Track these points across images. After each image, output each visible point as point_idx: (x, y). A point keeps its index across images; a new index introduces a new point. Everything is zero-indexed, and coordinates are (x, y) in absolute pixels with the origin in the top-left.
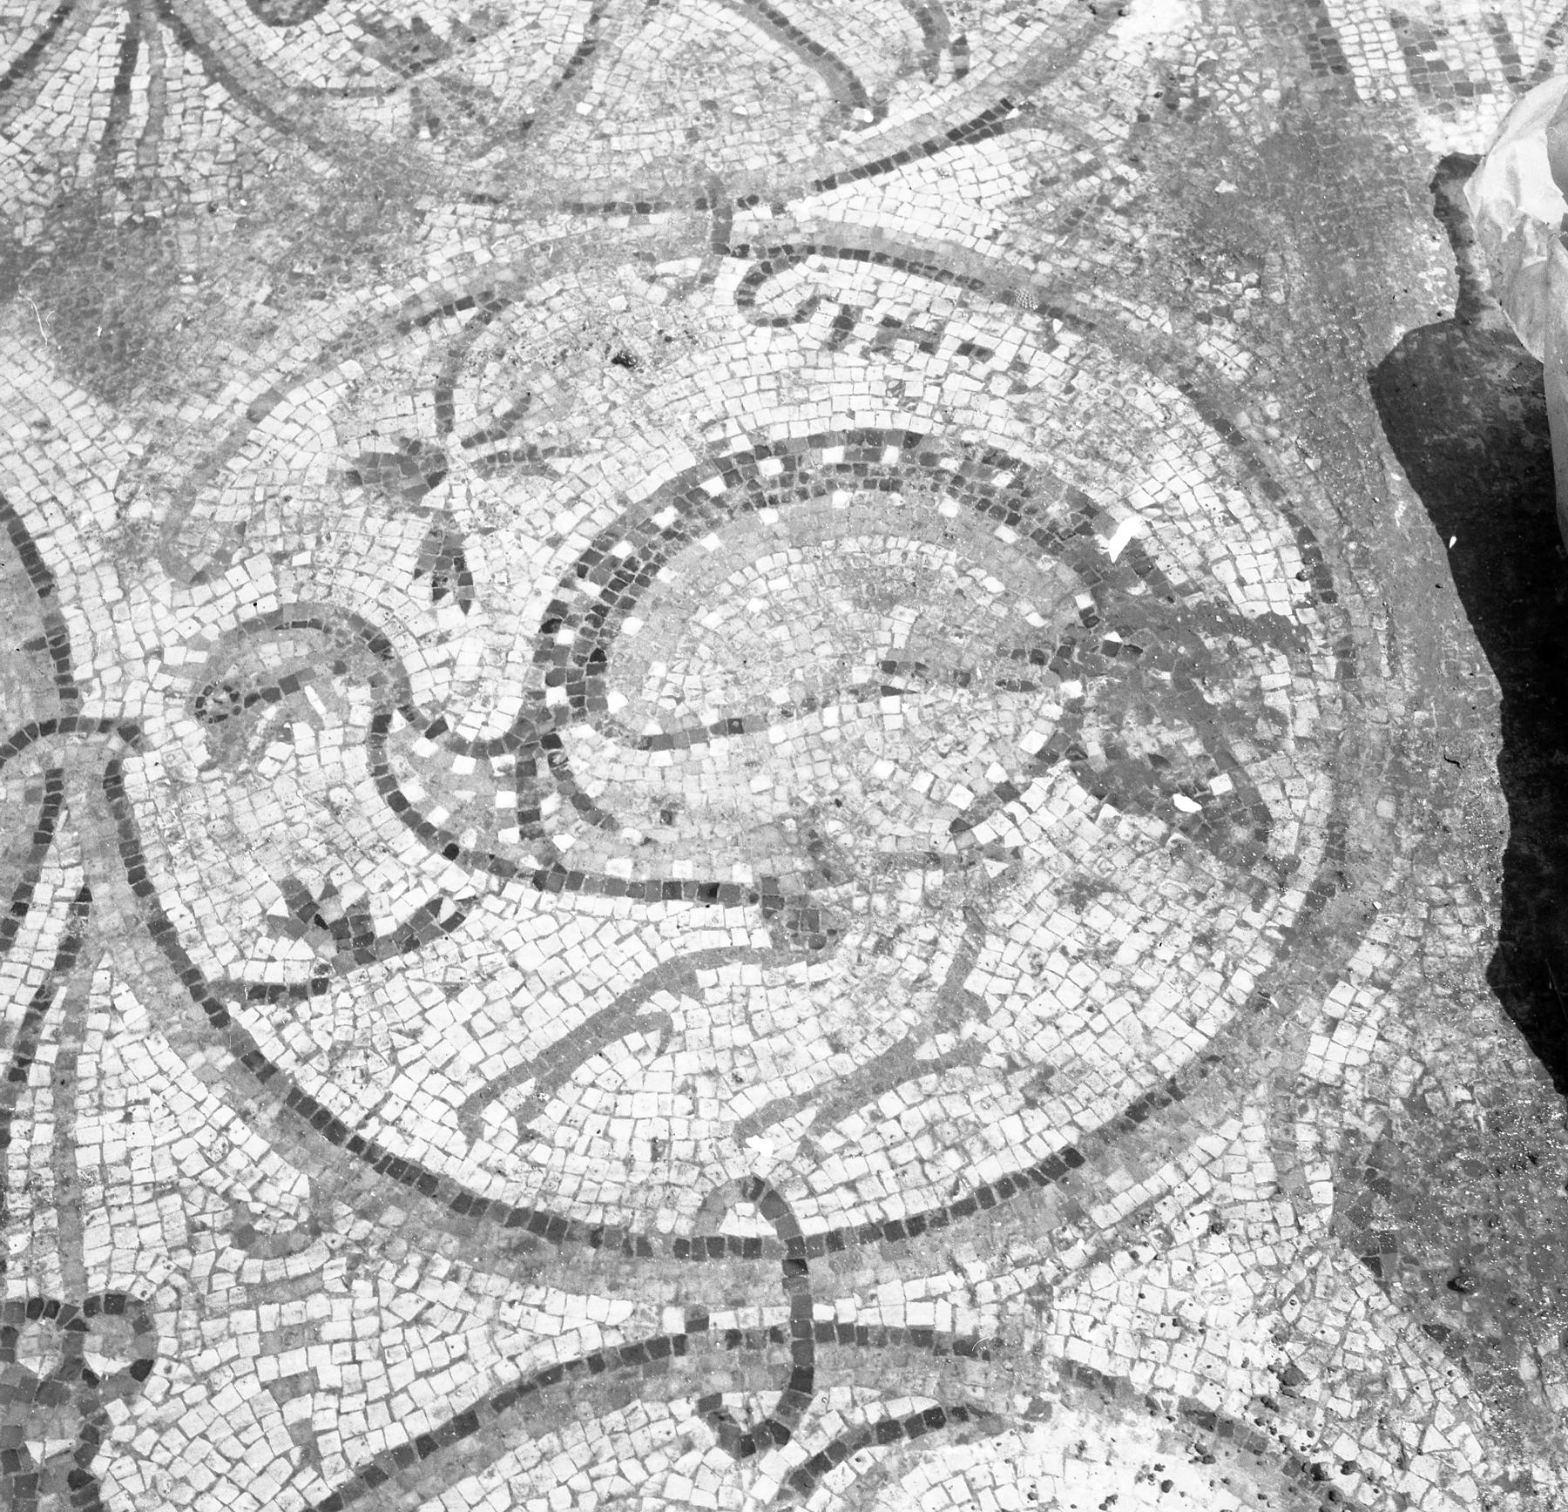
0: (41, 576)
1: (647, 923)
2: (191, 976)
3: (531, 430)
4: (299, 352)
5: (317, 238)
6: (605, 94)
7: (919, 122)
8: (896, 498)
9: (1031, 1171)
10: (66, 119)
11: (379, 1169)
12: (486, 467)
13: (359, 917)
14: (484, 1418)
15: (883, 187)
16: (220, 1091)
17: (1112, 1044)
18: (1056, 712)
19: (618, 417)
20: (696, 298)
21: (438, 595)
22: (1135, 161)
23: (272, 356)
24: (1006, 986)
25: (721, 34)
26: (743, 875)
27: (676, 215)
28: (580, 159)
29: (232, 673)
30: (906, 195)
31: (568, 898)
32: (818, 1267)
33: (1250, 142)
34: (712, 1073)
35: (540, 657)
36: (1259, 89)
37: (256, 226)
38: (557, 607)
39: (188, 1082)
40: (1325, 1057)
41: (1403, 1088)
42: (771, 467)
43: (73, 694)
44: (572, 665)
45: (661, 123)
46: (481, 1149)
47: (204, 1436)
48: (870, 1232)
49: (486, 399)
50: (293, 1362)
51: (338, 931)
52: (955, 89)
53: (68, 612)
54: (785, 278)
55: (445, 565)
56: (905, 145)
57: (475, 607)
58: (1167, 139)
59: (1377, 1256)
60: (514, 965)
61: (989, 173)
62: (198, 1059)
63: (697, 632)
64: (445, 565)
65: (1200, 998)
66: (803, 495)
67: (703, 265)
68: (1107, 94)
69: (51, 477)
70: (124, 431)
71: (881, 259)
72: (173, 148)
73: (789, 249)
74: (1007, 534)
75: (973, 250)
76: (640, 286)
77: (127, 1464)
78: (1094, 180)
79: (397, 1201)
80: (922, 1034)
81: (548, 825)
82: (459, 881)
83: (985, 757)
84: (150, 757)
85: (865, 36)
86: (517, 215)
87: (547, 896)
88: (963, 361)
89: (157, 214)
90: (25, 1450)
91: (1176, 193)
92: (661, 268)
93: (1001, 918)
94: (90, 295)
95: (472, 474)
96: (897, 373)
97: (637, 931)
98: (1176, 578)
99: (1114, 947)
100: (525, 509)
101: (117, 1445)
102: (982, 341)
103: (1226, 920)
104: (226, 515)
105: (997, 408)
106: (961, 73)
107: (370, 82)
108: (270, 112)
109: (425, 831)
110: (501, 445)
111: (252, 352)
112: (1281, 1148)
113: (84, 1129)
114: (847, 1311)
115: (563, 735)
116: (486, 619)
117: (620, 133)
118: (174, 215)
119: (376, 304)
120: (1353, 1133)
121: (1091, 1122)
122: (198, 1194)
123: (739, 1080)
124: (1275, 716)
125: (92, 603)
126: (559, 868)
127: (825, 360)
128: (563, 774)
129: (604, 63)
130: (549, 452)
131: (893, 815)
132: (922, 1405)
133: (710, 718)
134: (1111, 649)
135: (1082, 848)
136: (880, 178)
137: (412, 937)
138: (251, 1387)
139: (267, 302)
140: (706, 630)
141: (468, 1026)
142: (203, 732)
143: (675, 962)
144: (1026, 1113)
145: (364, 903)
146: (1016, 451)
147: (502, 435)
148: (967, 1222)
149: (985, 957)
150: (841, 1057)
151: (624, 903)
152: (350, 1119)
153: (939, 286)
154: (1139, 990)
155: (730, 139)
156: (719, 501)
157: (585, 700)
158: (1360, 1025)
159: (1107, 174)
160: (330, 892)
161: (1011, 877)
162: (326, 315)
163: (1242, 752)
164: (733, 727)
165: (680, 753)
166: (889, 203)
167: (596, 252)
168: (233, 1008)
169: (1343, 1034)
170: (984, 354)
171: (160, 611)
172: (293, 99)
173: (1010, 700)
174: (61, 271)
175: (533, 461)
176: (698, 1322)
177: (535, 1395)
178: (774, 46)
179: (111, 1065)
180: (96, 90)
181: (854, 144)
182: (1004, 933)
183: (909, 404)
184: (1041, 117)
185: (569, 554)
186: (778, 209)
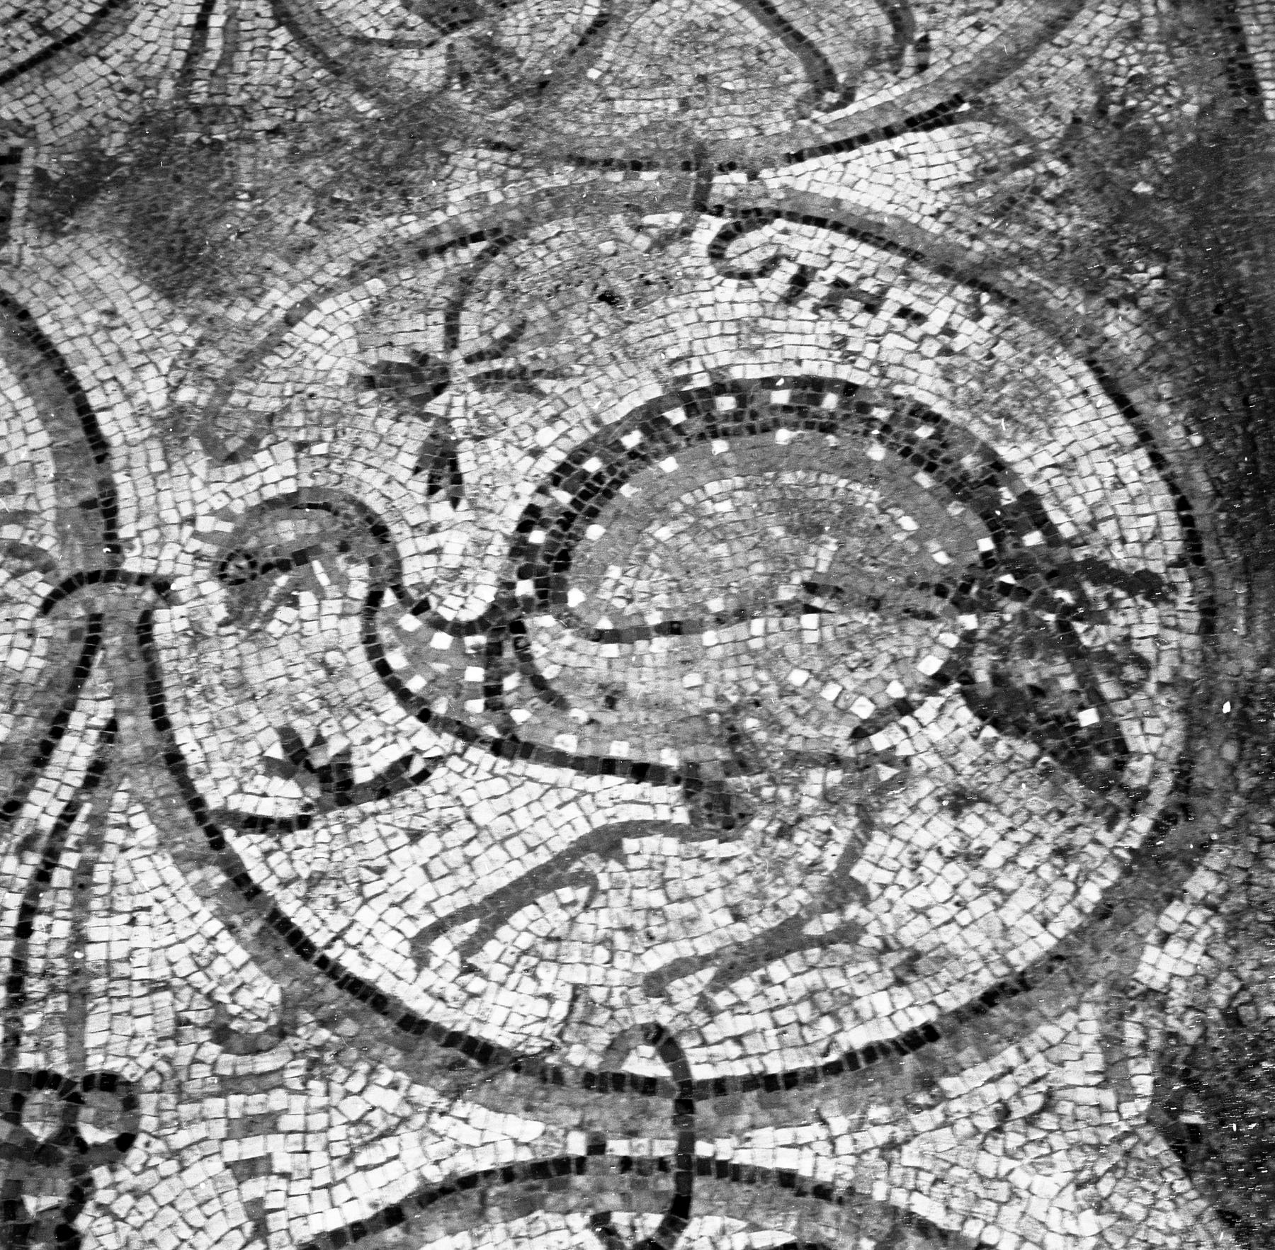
0: (99, 445)
1: (584, 793)
2: (197, 803)
3: (524, 353)
4: (333, 268)
5: (357, 169)
6: (612, 62)
7: (881, 108)
8: (831, 440)
9: (894, 1042)
10: (152, 48)
11: (340, 986)
12: (484, 382)
13: (342, 764)
15: (846, 163)
16: (212, 905)
17: (975, 937)
18: (952, 640)
19: (600, 348)
20: (676, 249)
21: (432, 490)
22: (1065, 159)
23: (310, 269)
24: (886, 877)
25: (718, 17)
26: (670, 759)
27: (666, 173)
28: (587, 118)
29: (252, 543)
30: (864, 172)
31: (520, 766)
32: (704, 1109)
33: (1167, 149)
34: (628, 930)
35: (515, 552)
36: (1181, 103)
37: (306, 156)
38: (532, 510)
39: (186, 895)
40: (1158, 966)
41: (1221, 999)
42: (726, 403)
43: (116, 549)
44: (540, 562)
45: (659, 91)
46: (427, 977)
47: (172, 1205)
48: (751, 1082)
49: (488, 322)
50: (253, 1147)
51: (323, 775)
52: (916, 83)
53: (119, 478)
54: (753, 238)
55: (440, 466)
56: (867, 128)
57: (463, 505)
58: (1096, 141)
59: (1186, 1144)
60: (469, 819)
61: (937, 159)
62: (196, 876)
63: (650, 542)
64: (440, 466)
65: (1053, 904)
66: (752, 430)
67: (684, 220)
68: (1047, 96)
69: (114, 359)
70: (179, 325)
71: (837, 227)
72: (240, 81)
73: (758, 211)
74: (924, 480)
75: (917, 225)
76: (627, 233)
77: (106, 1223)
78: (1029, 172)
79: (352, 1015)
80: (812, 912)
81: (509, 700)
83: (886, 674)
84: (178, 610)
85: (842, 28)
86: (530, 163)
87: (503, 762)
88: (900, 323)
89: (222, 137)
90: (21, 1203)
91: (1098, 190)
92: (648, 219)
93: (889, 818)
94: (161, 203)
95: (470, 387)
96: (842, 329)
97: (576, 799)
98: (1067, 531)
99: (984, 851)
100: (513, 422)
101: (99, 1206)
102: (919, 307)
103: (1081, 837)
104: (259, 405)
105: (927, 367)
106: (922, 67)
107: (410, 36)
108: (326, 57)
109: (404, 697)
110: (497, 364)
111: (292, 263)
112: (1110, 1041)
113: (96, 928)
114: (724, 1149)
115: (528, 622)
116: (471, 516)
117: (622, 98)
118: (237, 139)
119: (401, 230)
120: (1174, 1035)
121: (949, 1003)
122: (186, 992)
123: (651, 938)
124: (1142, 663)
125: (140, 472)
126: (514, 739)
127: (780, 313)
128: (525, 657)
129: (615, 34)
130: (538, 373)
131: (802, 718)
133: (654, 619)
134: (1005, 589)
135: (963, 761)
136: (843, 156)
138: (215, 1166)
139: (310, 222)
140: (658, 541)
141: (425, 867)
142: (224, 592)
143: (605, 829)
144: (894, 990)
145: (347, 753)
146: (939, 407)
147: (497, 356)
148: (835, 1081)
149: (872, 849)
150: (740, 926)
151: (568, 774)
152: (319, 940)
153: (885, 255)
154: (1001, 891)
155: (717, 111)
156: (678, 429)
157: (550, 595)
158: (1189, 940)
159: (1041, 169)
160: (320, 741)
161: (901, 782)
162: (359, 238)
163: (1109, 689)
164: (671, 628)
165: (626, 647)
166: (848, 178)
167: (593, 205)
168: (229, 834)
169: (1174, 947)
170: (919, 318)
171: (196, 484)
172: (346, 45)
173: (914, 627)
174: (137, 180)
175: (523, 382)
176: (597, 1147)
178: (762, 31)
179: (123, 874)
180: (179, 25)
181: (823, 124)
182: (889, 830)
183: (850, 358)
184: (988, 112)
185: (547, 465)
186: (753, 176)
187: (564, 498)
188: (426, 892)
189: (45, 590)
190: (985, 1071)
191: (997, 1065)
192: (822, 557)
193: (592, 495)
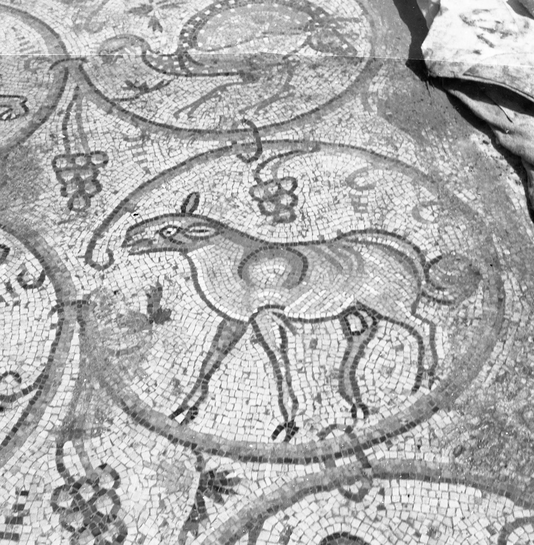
2: (106, 99)
8: (263, 5)
12: (163, 8)
14: (187, 163)
17: (324, 90)
18: (305, 38)
21: (154, 30)
26: (234, 70)
29: (106, 48)
31: (194, 78)
32: (261, 132)
34: (232, 103)
40: (372, 88)
46: (179, 120)
48: (272, 125)
59: (389, 118)
64: (155, 25)
65: (344, 81)
70: (72, 8)
74: (290, 9)
77: (105, 178)
80: (280, 93)
82: (167, 78)
98: (330, 13)
99: (323, 75)
103: (348, 68)
104: (100, 20)
109: (158, 70)
112: (365, 103)
113: (85, 125)
121: (321, 103)
124: (357, 35)
132: (288, 151)
133: (223, 45)
134: (317, 26)
151: (208, 78)
160: (136, 82)
163: (349, 40)
169: (377, 84)
173: (294, 37)
176: (234, 143)
179: (89, 114)
185: (185, 20)
187: (192, 26)
189: (50, 65)
190: (333, 114)
192: (266, 27)
193: (199, 25)
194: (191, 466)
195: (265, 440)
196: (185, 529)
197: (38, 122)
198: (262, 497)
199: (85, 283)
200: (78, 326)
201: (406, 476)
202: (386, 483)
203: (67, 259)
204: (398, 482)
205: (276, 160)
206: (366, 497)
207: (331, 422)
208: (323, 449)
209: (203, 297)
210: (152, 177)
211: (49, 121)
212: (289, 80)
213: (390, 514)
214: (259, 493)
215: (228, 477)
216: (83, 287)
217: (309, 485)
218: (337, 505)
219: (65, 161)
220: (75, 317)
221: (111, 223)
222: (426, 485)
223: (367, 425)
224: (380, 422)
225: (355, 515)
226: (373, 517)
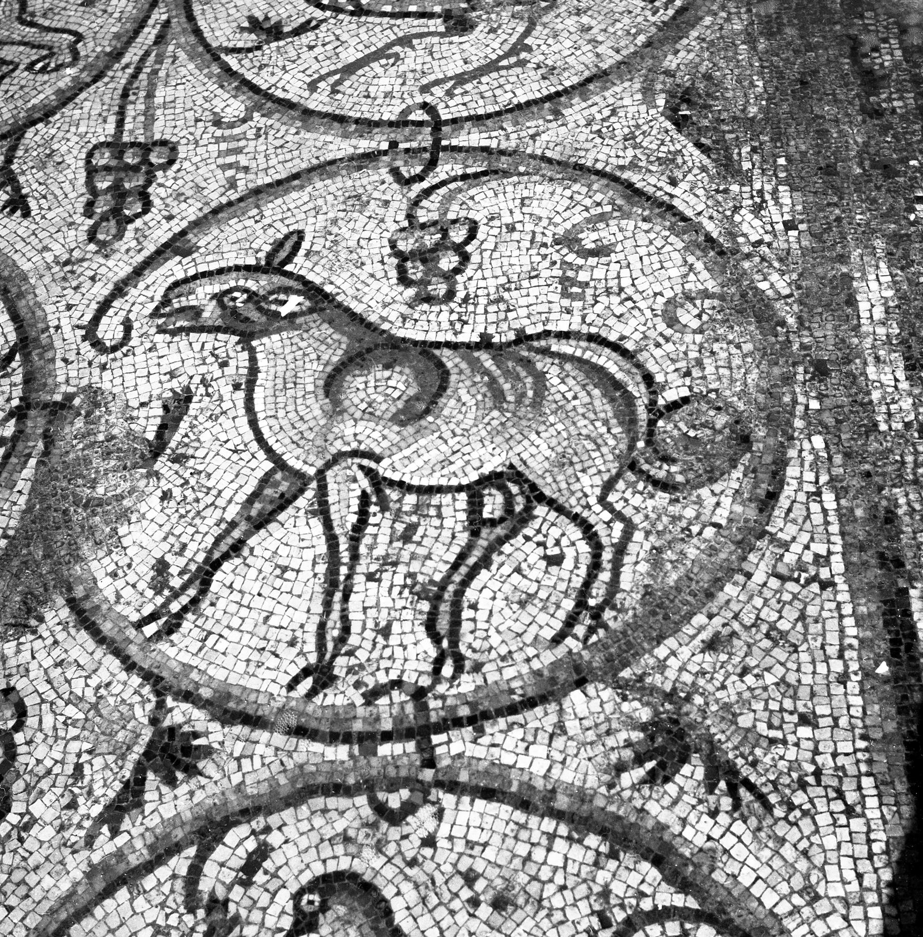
2: (207, 46)
13: (278, 26)
24: (541, 42)
26: (438, 9)
31: (363, 19)
40: (671, 62)
48: (469, 118)
50: (231, 159)
51: (268, 31)
62: (206, 71)
82: (319, 14)
114: (454, 142)
122: (200, 111)
132: (479, 170)
137: (297, 32)
138: (213, 166)
148: (509, 116)
158: (689, 52)
160: (267, 18)
168: (223, 56)
169: (682, 54)
176: (394, 145)
177: (325, 169)
182: (545, 25)
188: (316, 66)
190: (584, 105)
191: (590, 102)
194: (142, 714)
195: (274, 689)
196: (101, 820)
197: (88, 79)
198: (240, 788)
199: (73, 374)
200: (41, 445)
201: (488, 794)
202: (448, 800)
203: (58, 328)
204: (472, 802)
205: (452, 186)
206: (410, 819)
207: (393, 676)
208: (365, 720)
209: (253, 423)
210: (234, 197)
211: (106, 80)
212: (527, 33)
213: (440, 857)
214: (236, 779)
215: (196, 743)
216: (67, 381)
217: (321, 779)
218: (356, 824)
219: (107, 155)
220: (40, 431)
221: (146, 272)
222: (520, 817)
223: (454, 691)
224: (478, 688)
225: (379, 848)
226: (409, 855)
